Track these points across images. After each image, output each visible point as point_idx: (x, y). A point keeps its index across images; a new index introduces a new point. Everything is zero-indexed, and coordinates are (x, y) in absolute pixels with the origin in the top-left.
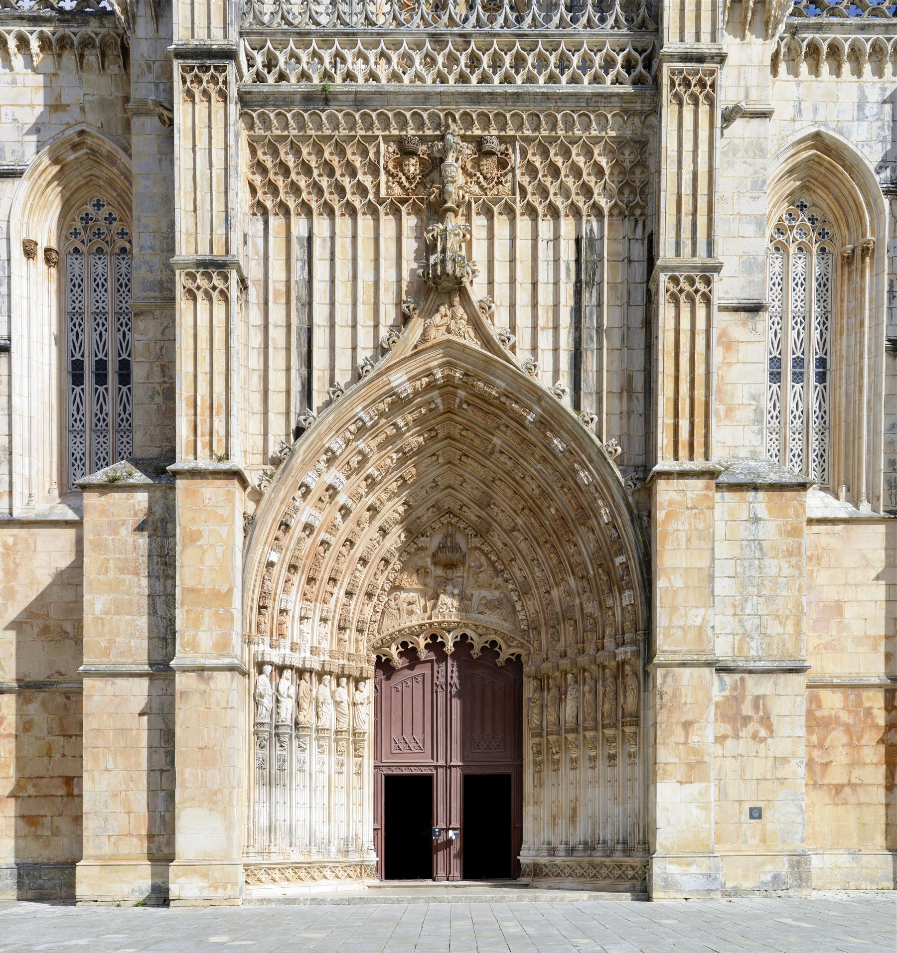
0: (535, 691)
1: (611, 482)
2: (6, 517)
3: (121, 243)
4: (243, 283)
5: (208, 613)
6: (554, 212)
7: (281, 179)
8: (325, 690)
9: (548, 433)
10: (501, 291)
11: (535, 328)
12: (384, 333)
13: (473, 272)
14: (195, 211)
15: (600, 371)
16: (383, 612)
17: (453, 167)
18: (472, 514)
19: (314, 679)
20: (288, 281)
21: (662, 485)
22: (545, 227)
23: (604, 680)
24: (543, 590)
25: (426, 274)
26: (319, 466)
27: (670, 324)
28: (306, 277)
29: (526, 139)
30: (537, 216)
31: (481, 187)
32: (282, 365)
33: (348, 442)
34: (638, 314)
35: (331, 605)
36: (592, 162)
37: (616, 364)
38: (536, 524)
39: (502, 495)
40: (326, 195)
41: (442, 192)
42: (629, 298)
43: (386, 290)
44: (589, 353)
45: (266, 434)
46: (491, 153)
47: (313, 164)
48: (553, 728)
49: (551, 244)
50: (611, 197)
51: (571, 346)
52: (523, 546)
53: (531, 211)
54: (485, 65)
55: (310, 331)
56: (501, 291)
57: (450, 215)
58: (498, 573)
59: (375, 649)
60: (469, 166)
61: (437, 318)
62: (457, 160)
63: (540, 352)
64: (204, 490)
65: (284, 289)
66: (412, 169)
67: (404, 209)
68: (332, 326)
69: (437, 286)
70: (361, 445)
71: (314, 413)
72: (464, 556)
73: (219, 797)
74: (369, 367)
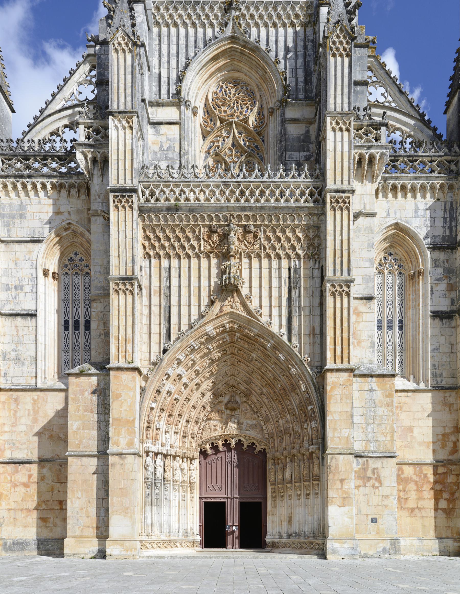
0: (272, 465)
1: (306, 373)
2: (34, 387)
3: (86, 270)
4: (140, 287)
5: (124, 430)
6: (279, 257)
7: (157, 243)
8: (177, 464)
9: (277, 352)
10: (255, 291)
11: (270, 306)
12: (203, 308)
13: (243, 282)
14: (119, 256)
15: (300, 325)
16: (203, 430)
17: (233, 237)
18: (243, 387)
19: (172, 459)
20: (160, 286)
21: (329, 375)
22: (275, 263)
23: (304, 460)
24: (275, 420)
25: (221, 283)
26: (174, 366)
27: (332, 305)
28: (168, 284)
29: (266, 226)
30: (271, 258)
31: (246, 246)
32: (158, 322)
33: (187, 356)
34: (317, 301)
35: (180, 426)
36: (295, 234)
37: (307, 322)
38: (272, 392)
39: (256, 379)
40: (177, 250)
41: (229, 248)
42: (313, 294)
43: (204, 290)
44: (295, 317)
45: (150, 352)
46: (250, 232)
47: (171, 237)
48: (280, 481)
49: (277, 270)
50: (304, 251)
51: (287, 314)
52: (266, 401)
53: (268, 256)
54: (247, 194)
55: (170, 307)
56: (255, 291)
57: (232, 258)
58: (255, 413)
59: (199, 446)
60: (240, 237)
61: (227, 302)
62: (235, 235)
63: (273, 317)
64: (122, 376)
65: (158, 290)
66: (215, 239)
67: (211, 256)
68: (180, 306)
69: (226, 288)
70: (193, 357)
71: (172, 343)
72: (239, 405)
73: (129, 511)
74: (196, 323)
